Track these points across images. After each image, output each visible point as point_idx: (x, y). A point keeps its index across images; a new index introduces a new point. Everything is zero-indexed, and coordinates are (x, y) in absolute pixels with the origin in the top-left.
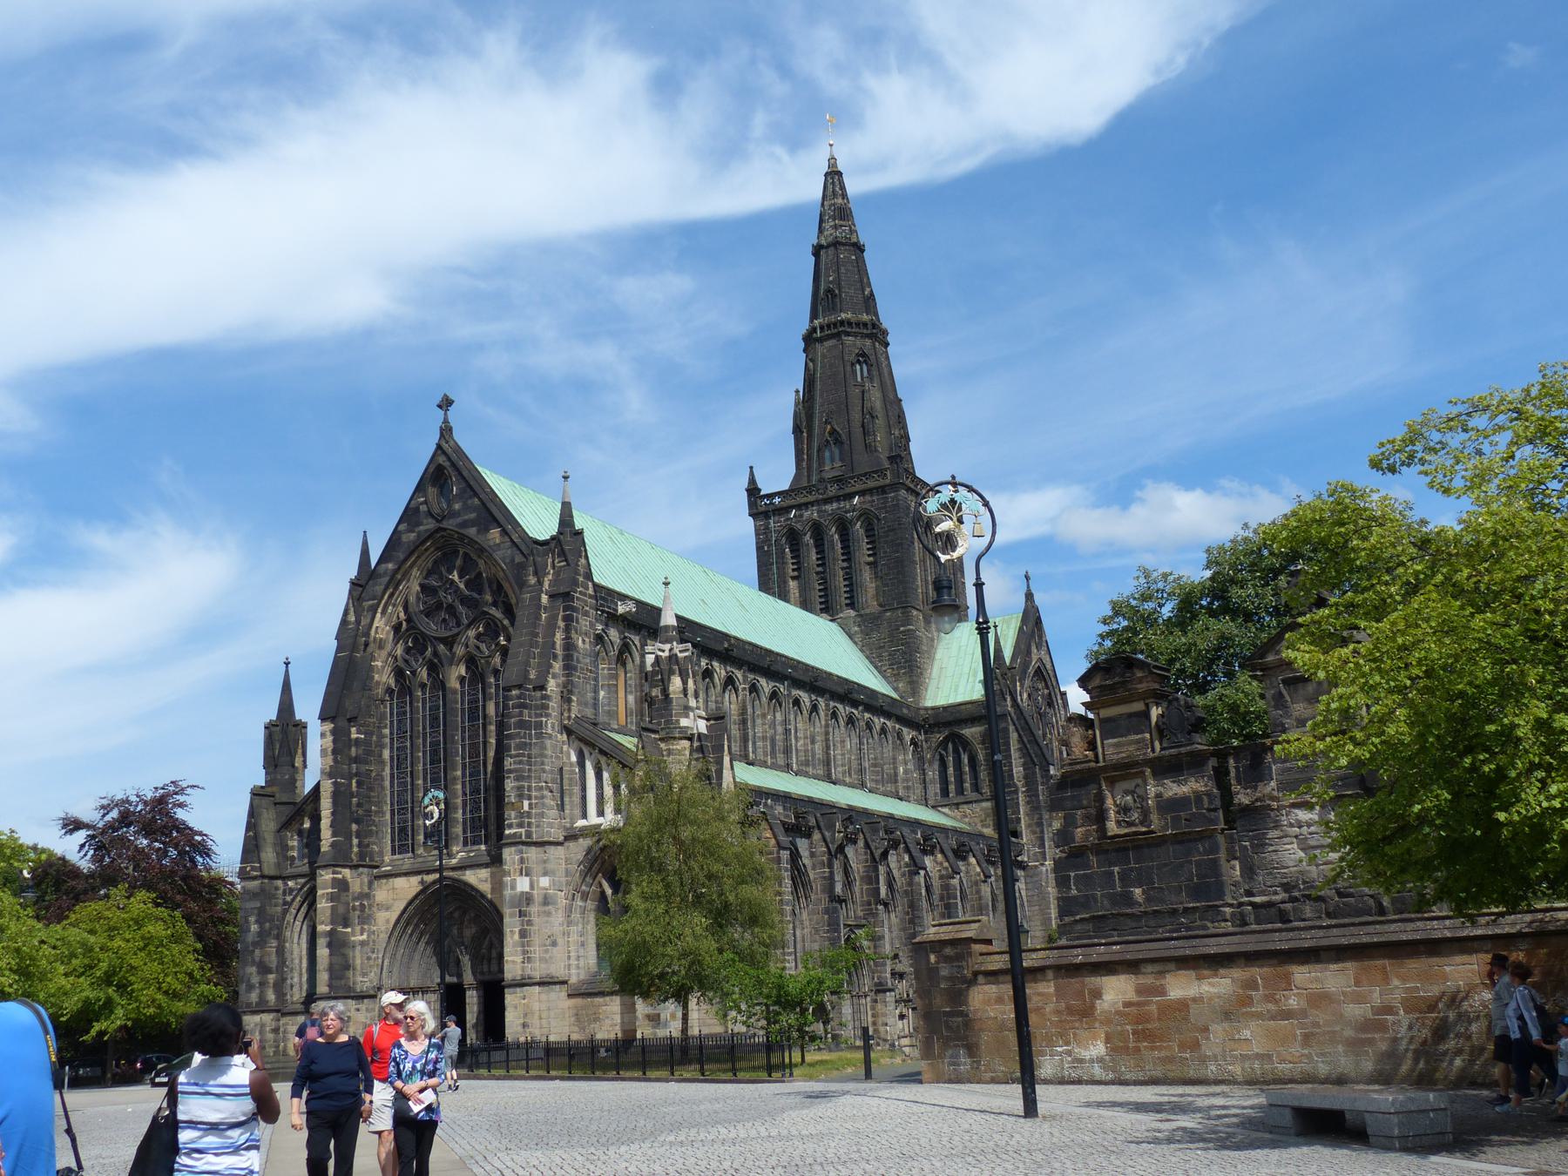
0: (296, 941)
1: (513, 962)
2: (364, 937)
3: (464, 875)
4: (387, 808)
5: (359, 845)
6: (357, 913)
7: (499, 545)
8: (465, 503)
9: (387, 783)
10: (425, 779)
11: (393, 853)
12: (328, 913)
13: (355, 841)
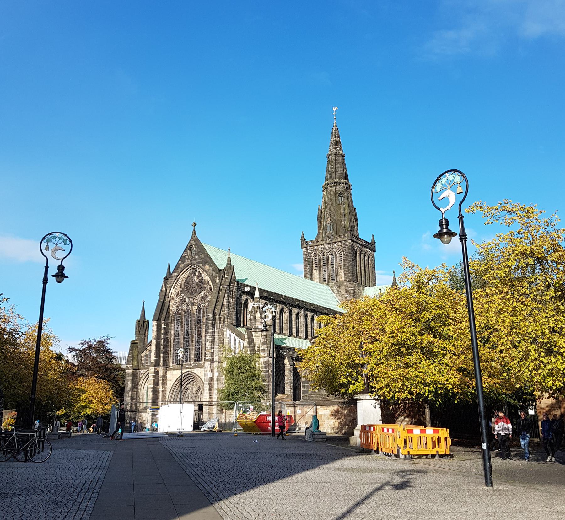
0: (142, 390)
1: (206, 398)
2: (163, 389)
3: (194, 371)
4: (172, 349)
5: (163, 360)
6: (161, 382)
7: (208, 270)
8: (199, 256)
9: (172, 341)
10: (184, 340)
11: (173, 363)
12: (152, 381)
13: (162, 359)
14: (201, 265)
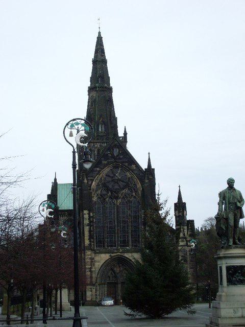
11: (97, 247)
14: (126, 164)
